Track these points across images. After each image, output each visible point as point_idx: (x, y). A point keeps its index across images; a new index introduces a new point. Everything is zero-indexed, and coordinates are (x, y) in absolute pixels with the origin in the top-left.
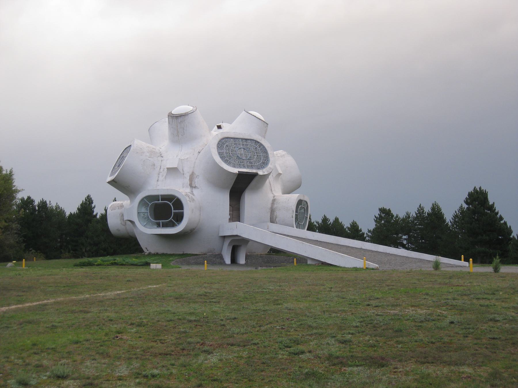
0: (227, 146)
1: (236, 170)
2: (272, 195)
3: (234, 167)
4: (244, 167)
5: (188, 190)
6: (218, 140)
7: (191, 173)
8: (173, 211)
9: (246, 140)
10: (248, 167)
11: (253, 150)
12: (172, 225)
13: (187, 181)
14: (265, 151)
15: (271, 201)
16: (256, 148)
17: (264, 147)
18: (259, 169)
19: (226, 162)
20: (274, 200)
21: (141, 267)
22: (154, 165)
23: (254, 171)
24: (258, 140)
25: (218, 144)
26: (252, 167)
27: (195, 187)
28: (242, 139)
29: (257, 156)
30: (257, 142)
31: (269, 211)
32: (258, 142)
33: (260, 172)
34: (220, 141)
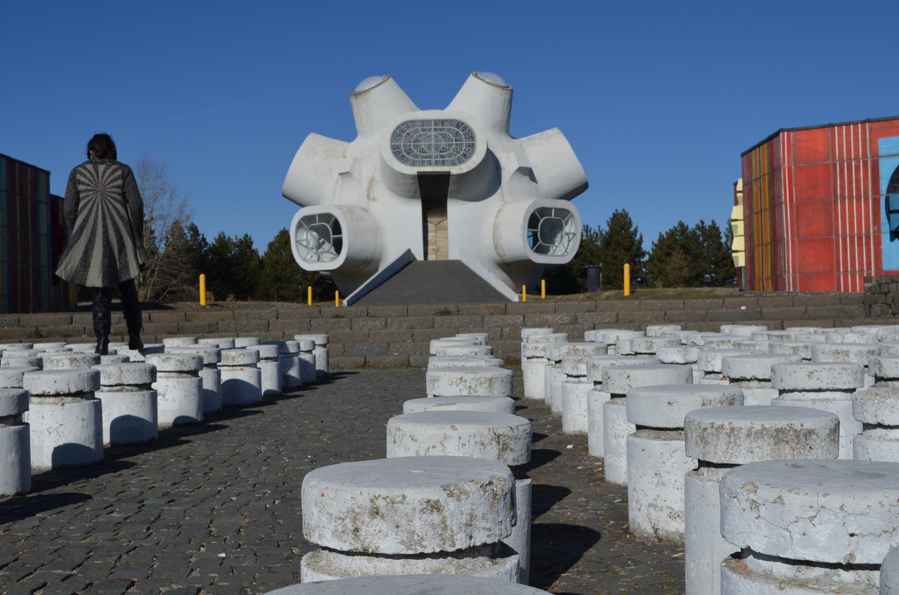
0: (408, 134)
1: (413, 171)
3: (413, 164)
4: (430, 164)
7: (370, 178)
8: (332, 236)
9: (443, 122)
10: (436, 163)
11: (451, 135)
14: (471, 136)
15: (495, 213)
16: (457, 133)
17: (470, 131)
18: (454, 164)
24: (462, 119)
25: (395, 132)
26: (443, 163)
27: (374, 199)
28: (436, 122)
29: (457, 145)
30: (459, 124)
33: (455, 170)
34: (398, 128)
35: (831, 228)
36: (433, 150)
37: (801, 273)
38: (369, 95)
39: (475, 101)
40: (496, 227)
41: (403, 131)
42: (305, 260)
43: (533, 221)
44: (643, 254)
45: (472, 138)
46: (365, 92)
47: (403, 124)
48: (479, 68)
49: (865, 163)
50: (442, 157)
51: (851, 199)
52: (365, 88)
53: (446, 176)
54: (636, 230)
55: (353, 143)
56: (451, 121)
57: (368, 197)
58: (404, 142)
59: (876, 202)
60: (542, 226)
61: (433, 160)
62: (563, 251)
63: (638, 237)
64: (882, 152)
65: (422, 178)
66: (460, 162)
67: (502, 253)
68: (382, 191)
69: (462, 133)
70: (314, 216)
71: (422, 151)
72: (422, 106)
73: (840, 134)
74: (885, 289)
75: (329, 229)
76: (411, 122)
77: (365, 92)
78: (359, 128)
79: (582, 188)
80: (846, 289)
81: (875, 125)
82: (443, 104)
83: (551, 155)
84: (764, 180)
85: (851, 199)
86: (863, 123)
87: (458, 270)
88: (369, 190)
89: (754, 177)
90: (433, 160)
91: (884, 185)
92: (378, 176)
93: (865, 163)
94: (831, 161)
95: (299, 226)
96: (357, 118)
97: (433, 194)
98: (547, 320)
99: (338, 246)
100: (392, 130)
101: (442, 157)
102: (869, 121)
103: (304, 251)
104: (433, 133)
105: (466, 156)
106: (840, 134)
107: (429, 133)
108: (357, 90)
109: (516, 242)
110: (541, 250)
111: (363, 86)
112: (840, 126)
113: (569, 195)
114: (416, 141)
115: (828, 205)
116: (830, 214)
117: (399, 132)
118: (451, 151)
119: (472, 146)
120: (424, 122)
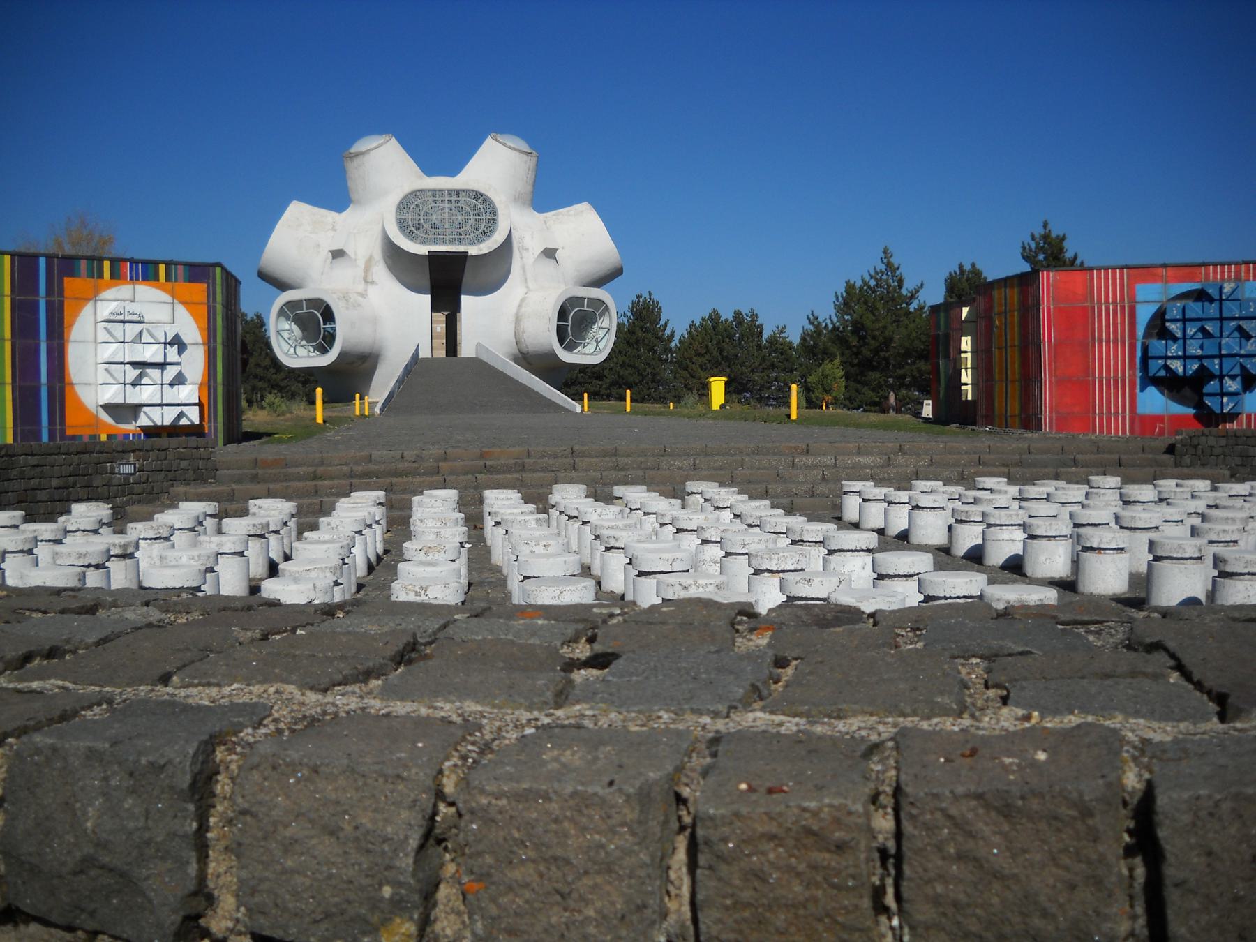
1: (423, 250)
2: (525, 290)
3: (423, 243)
4: (443, 242)
5: (360, 287)
6: (402, 196)
9: (458, 192)
12: (323, 350)
13: (361, 273)
15: (517, 302)
17: (491, 203)
18: (473, 243)
19: (410, 235)
20: (522, 300)
21: (262, 430)
22: (318, 246)
23: (461, 248)
25: (401, 202)
27: (373, 282)
28: (450, 191)
30: (478, 195)
31: (512, 319)
32: (482, 195)
33: (473, 251)
34: (405, 198)
35: (1087, 370)
36: (447, 226)
37: (1057, 412)
38: (367, 157)
39: (496, 167)
40: (518, 320)
41: (411, 202)
42: (287, 354)
43: (562, 314)
44: (668, 350)
45: (494, 212)
46: (362, 153)
47: (411, 193)
48: (501, 128)
49: (1123, 309)
50: (458, 234)
51: (1108, 342)
52: (363, 149)
53: (463, 256)
54: (666, 323)
55: (344, 214)
56: (468, 191)
57: (366, 281)
58: (413, 212)
59: (1133, 347)
60: (573, 320)
61: (447, 238)
62: (596, 349)
63: (668, 332)
64: (1139, 297)
65: (433, 256)
66: (480, 240)
67: (525, 350)
68: (381, 272)
69: (481, 208)
70: (301, 301)
71: (434, 226)
72: (429, 170)
73: (1099, 278)
74: (1195, 442)
75: (317, 320)
76: (421, 191)
77: (362, 153)
78: (353, 196)
79: (617, 273)
80: (1101, 431)
81: (1132, 271)
82: (454, 170)
83: (580, 236)
84: (1013, 316)
85: (1108, 342)
86: (1122, 268)
87: (479, 367)
88: (367, 269)
89: (996, 310)
90: (447, 238)
91: (1140, 331)
92: (377, 252)
93: (1123, 309)
94: (1088, 304)
95: (281, 313)
96: (350, 184)
97: (446, 281)
98: (859, 463)
99: (330, 338)
100: (397, 201)
101: (458, 234)
102: (1128, 267)
103: (285, 347)
104: (447, 205)
105: (486, 234)
106: (1099, 278)
107: (442, 206)
108: (352, 150)
109: (542, 333)
110: (570, 348)
111: (359, 147)
112: (1099, 269)
113: (599, 282)
114: (426, 214)
115: (1085, 348)
116: (1087, 356)
117: (405, 204)
118: (468, 227)
119: (493, 222)
120: (435, 192)
